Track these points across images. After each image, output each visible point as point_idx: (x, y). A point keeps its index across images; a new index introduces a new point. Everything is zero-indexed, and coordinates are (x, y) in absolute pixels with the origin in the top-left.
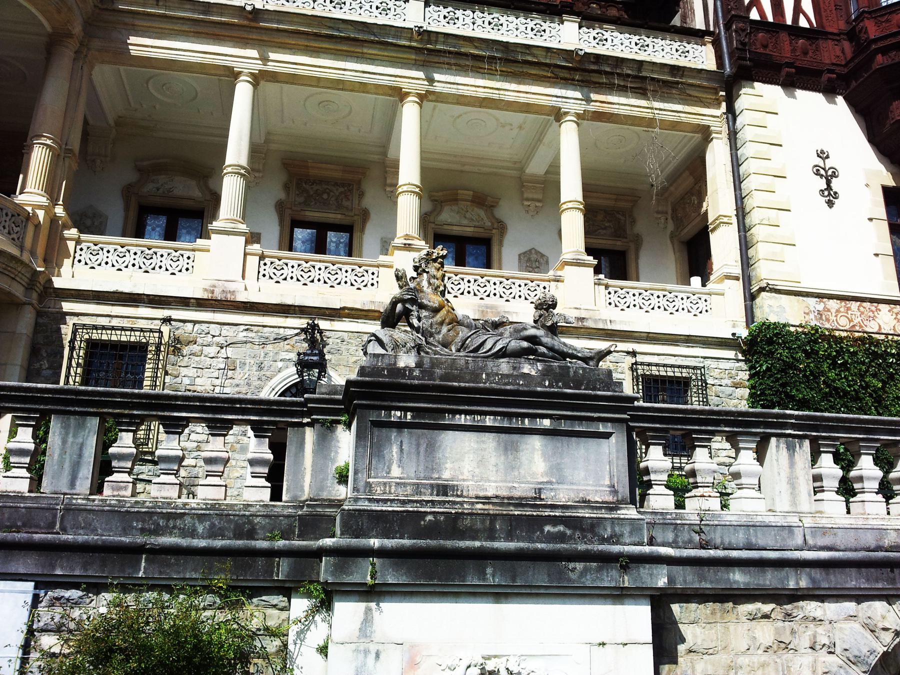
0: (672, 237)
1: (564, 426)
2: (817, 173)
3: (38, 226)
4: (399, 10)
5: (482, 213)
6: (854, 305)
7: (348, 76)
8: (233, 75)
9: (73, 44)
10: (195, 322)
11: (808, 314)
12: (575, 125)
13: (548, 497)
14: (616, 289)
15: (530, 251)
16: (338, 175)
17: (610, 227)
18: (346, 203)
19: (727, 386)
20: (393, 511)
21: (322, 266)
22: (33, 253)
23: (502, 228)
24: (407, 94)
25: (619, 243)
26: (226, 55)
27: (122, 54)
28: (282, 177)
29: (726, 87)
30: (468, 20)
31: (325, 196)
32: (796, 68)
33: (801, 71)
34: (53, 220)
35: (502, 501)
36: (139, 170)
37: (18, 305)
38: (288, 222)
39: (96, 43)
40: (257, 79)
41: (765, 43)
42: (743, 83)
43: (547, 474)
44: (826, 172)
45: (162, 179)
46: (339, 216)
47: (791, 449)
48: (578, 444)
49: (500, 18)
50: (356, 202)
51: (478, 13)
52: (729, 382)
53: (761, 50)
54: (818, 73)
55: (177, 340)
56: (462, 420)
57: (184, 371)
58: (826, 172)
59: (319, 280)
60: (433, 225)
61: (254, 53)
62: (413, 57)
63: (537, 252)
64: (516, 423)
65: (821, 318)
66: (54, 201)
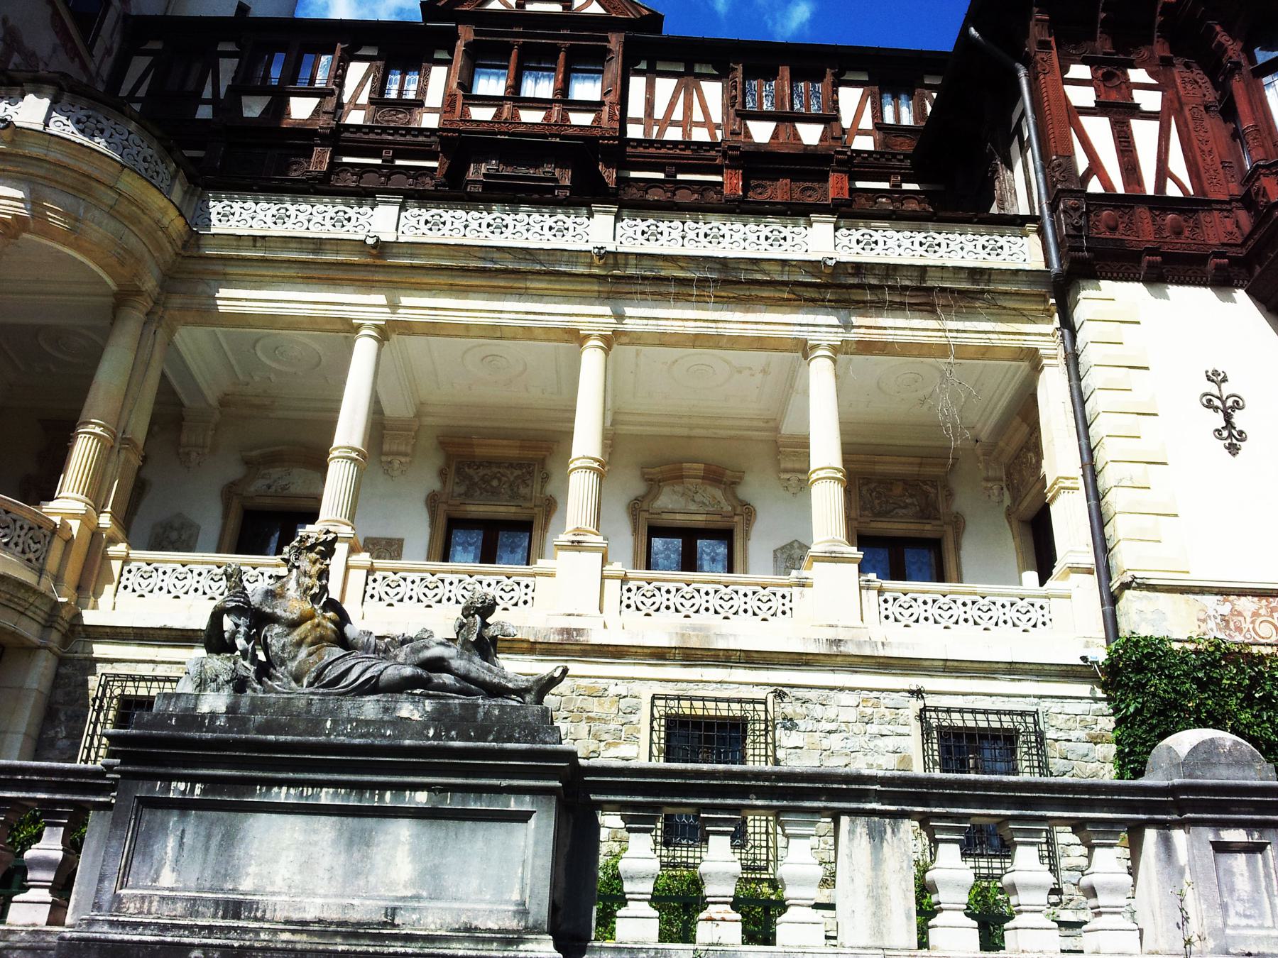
0: (1009, 513)
2: (1209, 405)
3: (69, 542)
4: (579, 229)
5: (718, 493)
7: (506, 320)
8: (351, 328)
9: (144, 304)
11: (1204, 621)
12: (829, 362)
13: (407, 922)
14: (896, 595)
15: (791, 545)
16: (514, 453)
17: (913, 504)
18: (523, 491)
19: (1078, 740)
20: (140, 942)
21: (455, 578)
22: (58, 579)
23: (748, 512)
24: (587, 337)
25: (928, 527)
26: (343, 304)
27: (208, 314)
28: (437, 461)
29: (1058, 291)
30: (676, 234)
31: (495, 483)
32: (1162, 254)
33: (1169, 258)
34: (96, 533)
35: (326, 928)
37: (30, 650)
38: (442, 522)
39: (177, 301)
40: (384, 333)
41: (1112, 223)
42: (1083, 283)
43: (413, 883)
44: (1224, 403)
45: (276, 472)
46: (513, 509)
47: (876, 836)
48: (473, 830)
49: (722, 227)
50: (537, 487)
51: (690, 224)
52: (1082, 734)
53: (1108, 235)
54: (1202, 260)
58: (1224, 403)
59: (449, 599)
60: (646, 515)
61: (380, 299)
62: (596, 288)
66: (99, 510)
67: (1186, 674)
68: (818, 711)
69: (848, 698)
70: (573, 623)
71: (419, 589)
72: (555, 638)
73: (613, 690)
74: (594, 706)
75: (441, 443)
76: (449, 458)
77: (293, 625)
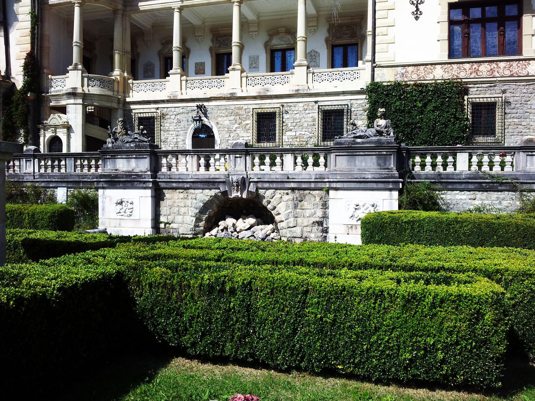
1: (138, 157)
3: (118, 82)
5: (290, 37)
6: (422, 68)
9: (120, 12)
10: (167, 108)
11: (396, 75)
15: (311, 51)
22: (118, 91)
25: (353, 40)
27: (137, 10)
34: (124, 78)
36: (162, 44)
39: (128, 9)
40: (181, 9)
55: (163, 114)
56: (119, 157)
57: (166, 125)
63: (315, 51)
64: (129, 157)
65: (403, 76)
66: (124, 72)
67: (382, 93)
68: (293, 108)
69: (301, 105)
70: (234, 91)
71: (198, 85)
72: (229, 96)
73: (244, 108)
74: (240, 112)
75: (211, 31)
76: (213, 35)
77: (119, 133)
